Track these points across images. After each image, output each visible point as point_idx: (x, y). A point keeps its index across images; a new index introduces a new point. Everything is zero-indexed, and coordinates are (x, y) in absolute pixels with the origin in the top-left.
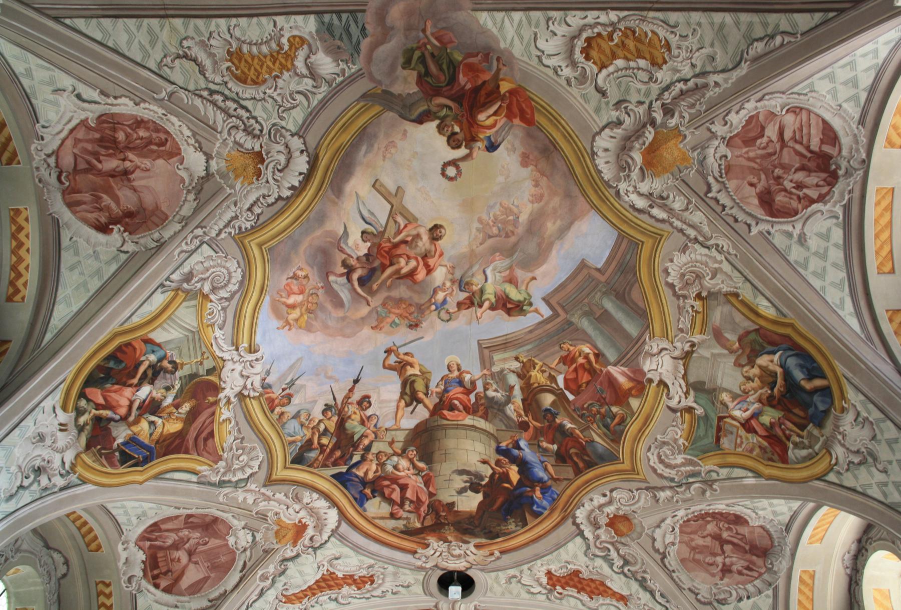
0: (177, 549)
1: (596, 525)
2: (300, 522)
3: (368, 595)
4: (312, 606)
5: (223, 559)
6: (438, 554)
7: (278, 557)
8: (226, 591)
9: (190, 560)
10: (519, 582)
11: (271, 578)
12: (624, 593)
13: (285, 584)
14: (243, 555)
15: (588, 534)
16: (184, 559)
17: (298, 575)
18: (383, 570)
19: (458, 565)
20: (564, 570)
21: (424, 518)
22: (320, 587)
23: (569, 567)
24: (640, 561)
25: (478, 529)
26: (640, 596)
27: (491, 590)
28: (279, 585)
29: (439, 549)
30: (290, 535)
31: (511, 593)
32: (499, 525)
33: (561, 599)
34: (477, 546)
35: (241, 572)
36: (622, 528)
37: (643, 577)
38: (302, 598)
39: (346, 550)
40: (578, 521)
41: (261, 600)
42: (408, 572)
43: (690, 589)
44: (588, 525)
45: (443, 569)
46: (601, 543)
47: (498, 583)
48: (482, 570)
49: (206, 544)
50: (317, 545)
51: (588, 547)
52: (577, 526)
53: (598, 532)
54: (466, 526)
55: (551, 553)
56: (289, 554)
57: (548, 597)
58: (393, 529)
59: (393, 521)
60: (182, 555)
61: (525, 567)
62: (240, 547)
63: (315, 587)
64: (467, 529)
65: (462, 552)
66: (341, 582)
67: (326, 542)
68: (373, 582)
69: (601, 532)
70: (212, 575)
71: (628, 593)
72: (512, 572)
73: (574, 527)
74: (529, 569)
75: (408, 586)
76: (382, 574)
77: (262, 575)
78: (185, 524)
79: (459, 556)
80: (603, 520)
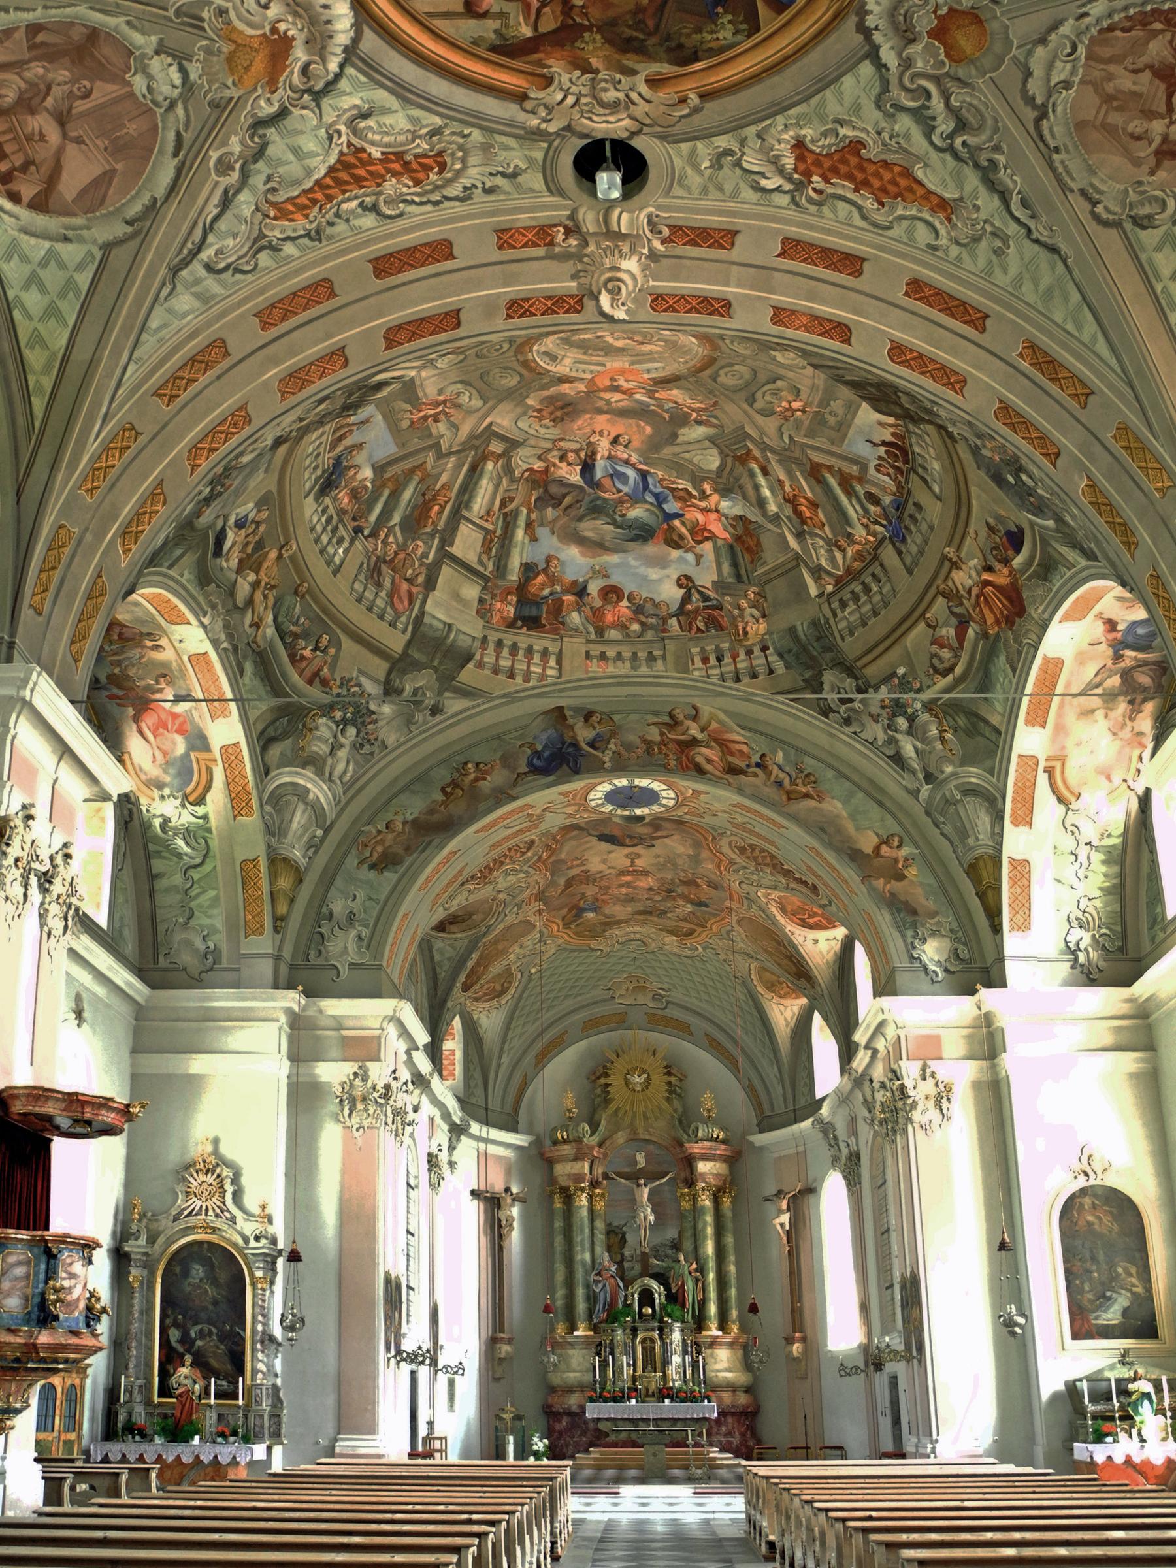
0: (33, 112)
1: (907, 36)
2: (274, 30)
3: (436, 197)
4: (331, 224)
5: (132, 128)
6: (570, 100)
7: (244, 118)
8: (155, 200)
9: (65, 135)
10: (738, 164)
11: (238, 166)
12: (947, 195)
13: (269, 178)
14: (171, 117)
15: (888, 56)
16: (54, 135)
17: (291, 157)
18: (461, 141)
19: (613, 126)
20: (831, 140)
21: (538, 12)
22: (339, 182)
23: (843, 131)
24: (990, 122)
25: (652, 41)
26: (979, 203)
27: (680, 181)
28: (258, 181)
29: (574, 89)
30: (259, 64)
31: (720, 189)
32: (699, 30)
33: (820, 204)
34: (654, 82)
35: (175, 155)
36: (963, 42)
37: (991, 161)
38: (306, 207)
39: (382, 96)
40: (871, 22)
41: (228, 215)
42: (511, 142)
43: (1083, 192)
44: (891, 34)
45: (586, 136)
46: (912, 78)
47: (696, 166)
48: (663, 137)
49: (87, 95)
50: (320, 85)
51: (885, 88)
52: (866, 32)
53: (912, 50)
54: (629, 32)
55: (806, 99)
56: (267, 109)
57: (794, 201)
58: (475, 43)
59: (472, 23)
60: (41, 122)
61: (752, 130)
62: (160, 98)
63: (328, 181)
64: (629, 40)
65: (621, 95)
66: (378, 168)
67: (338, 77)
68: (443, 167)
69: (916, 49)
70: (119, 166)
71: (957, 196)
72: (722, 142)
73: (861, 37)
74: (759, 136)
75: (514, 175)
76: (461, 148)
77: (220, 160)
78: (31, 48)
79: (614, 106)
80: (924, 22)
